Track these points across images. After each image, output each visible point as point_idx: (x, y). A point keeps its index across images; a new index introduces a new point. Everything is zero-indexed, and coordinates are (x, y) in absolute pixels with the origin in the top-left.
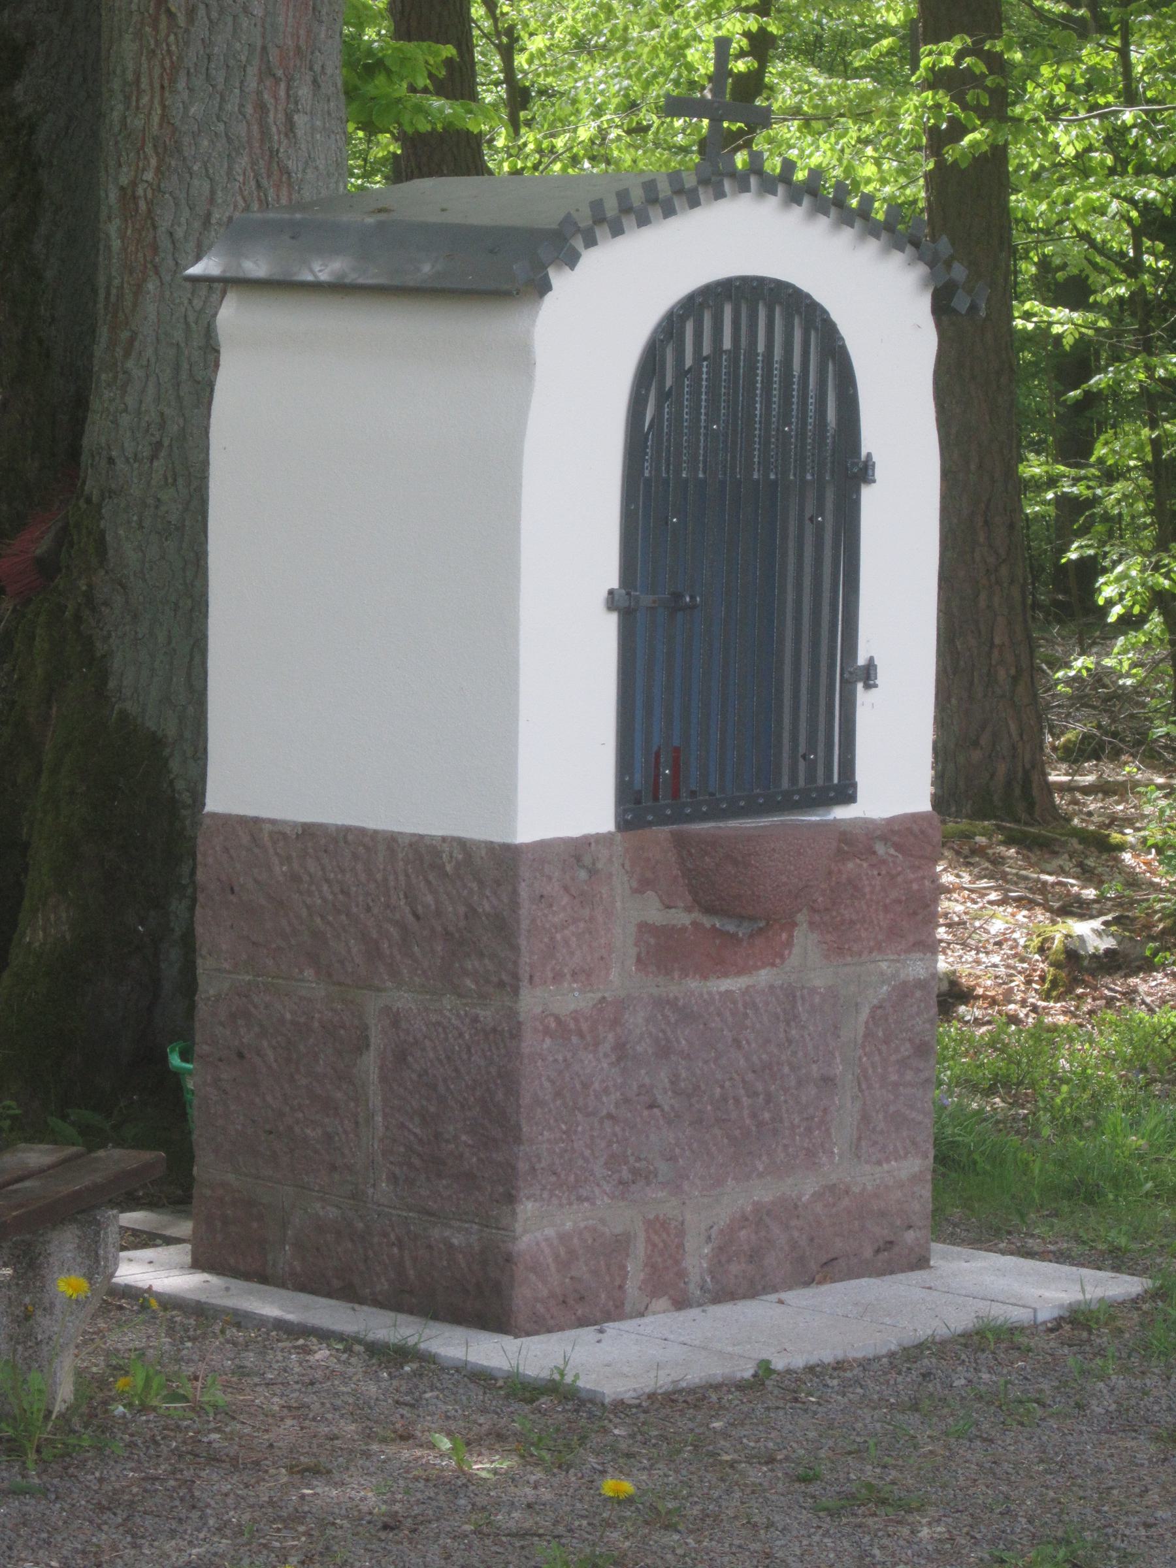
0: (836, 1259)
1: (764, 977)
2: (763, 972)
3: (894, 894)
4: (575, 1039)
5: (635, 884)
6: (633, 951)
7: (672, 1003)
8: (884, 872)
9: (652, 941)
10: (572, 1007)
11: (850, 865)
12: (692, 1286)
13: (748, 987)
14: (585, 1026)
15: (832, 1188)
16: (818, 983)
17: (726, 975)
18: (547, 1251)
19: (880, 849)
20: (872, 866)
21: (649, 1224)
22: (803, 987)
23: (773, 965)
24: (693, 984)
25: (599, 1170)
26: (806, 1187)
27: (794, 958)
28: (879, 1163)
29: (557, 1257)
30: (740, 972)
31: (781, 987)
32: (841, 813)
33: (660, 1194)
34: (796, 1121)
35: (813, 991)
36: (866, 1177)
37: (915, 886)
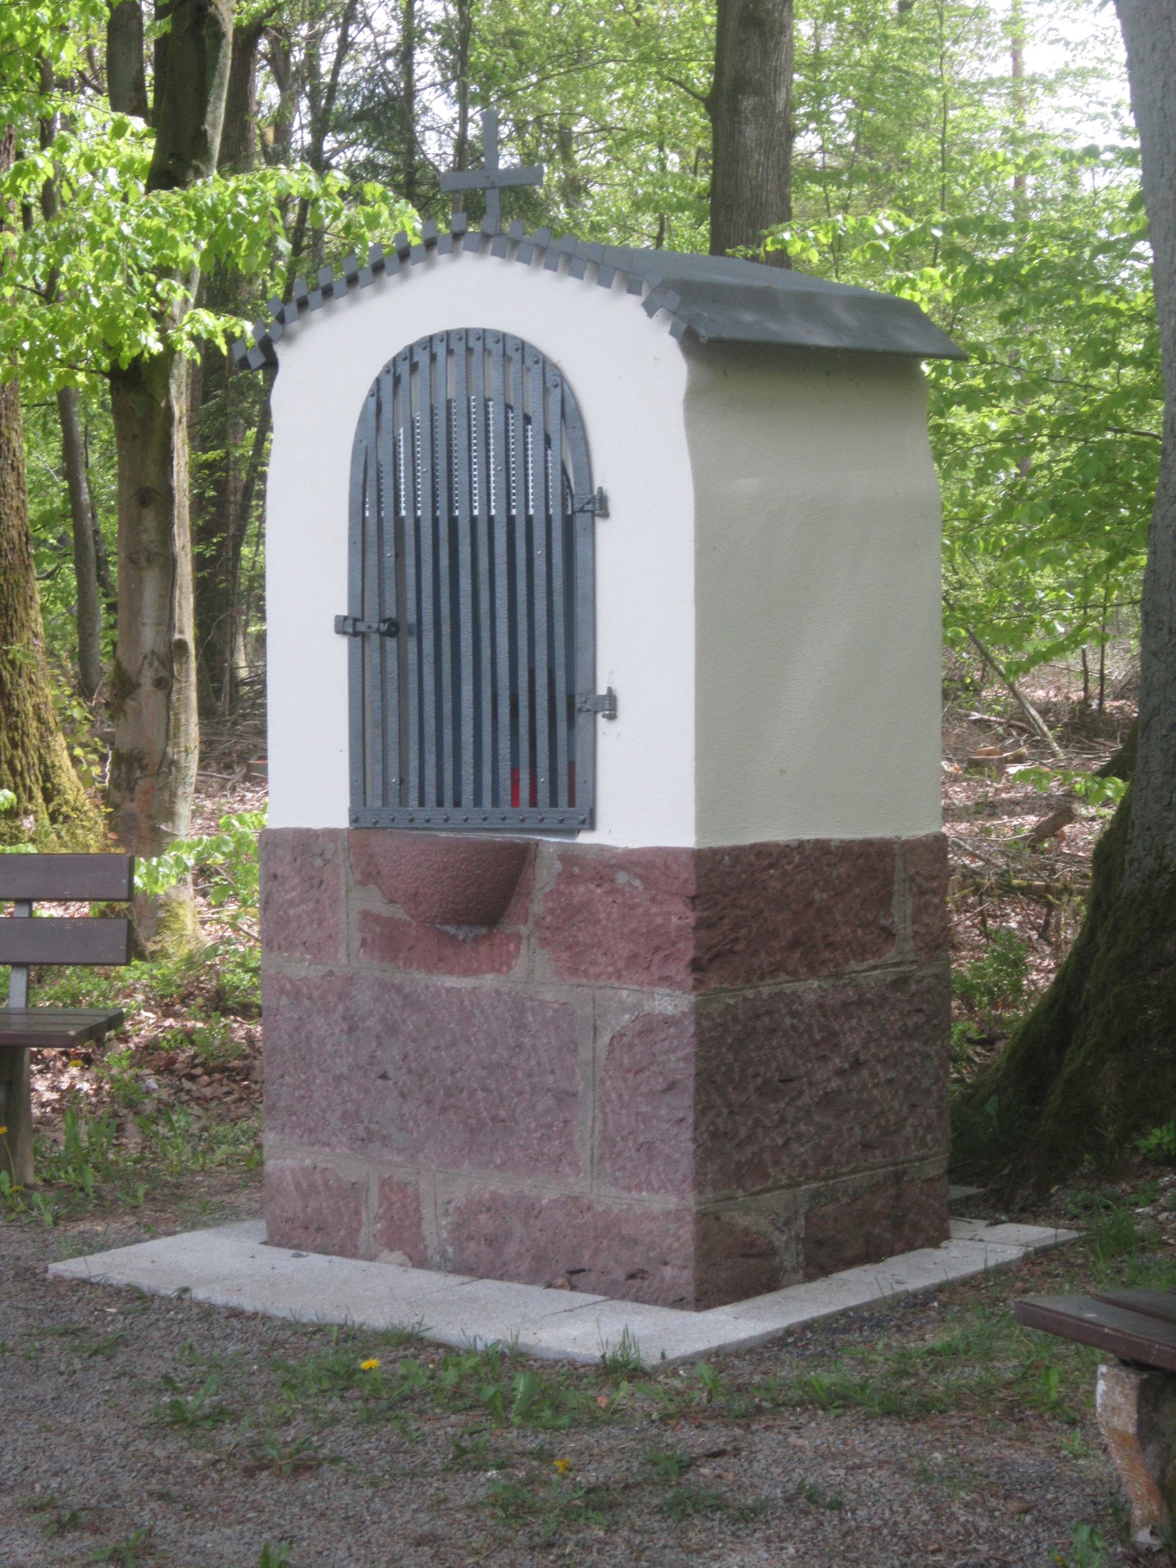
0: (582, 1270)
1: (489, 981)
2: (489, 977)
3: (633, 925)
4: (307, 1003)
5: (358, 877)
6: (358, 936)
7: (399, 989)
8: (620, 901)
9: (378, 929)
10: (303, 974)
11: (582, 889)
12: (430, 1251)
13: (475, 988)
14: (316, 994)
15: (575, 1199)
16: (548, 997)
17: (450, 972)
18: (289, 1178)
19: (622, 878)
20: (608, 893)
21: (385, 1183)
22: (531, 999)
23: (499, 971)
24: (419, 976)
25: (334, 1118)
26: (549, 1193)
27: (520, 966)
28: (628, 1189)
29: (298, 1186)
30: (465, 972)
31: (509, 994)
32: (584, 838)
33: (395, 1159)
34: (533, 1125)
35: (543, 1004)
36: (608, 1197)
37: (659, 921)
